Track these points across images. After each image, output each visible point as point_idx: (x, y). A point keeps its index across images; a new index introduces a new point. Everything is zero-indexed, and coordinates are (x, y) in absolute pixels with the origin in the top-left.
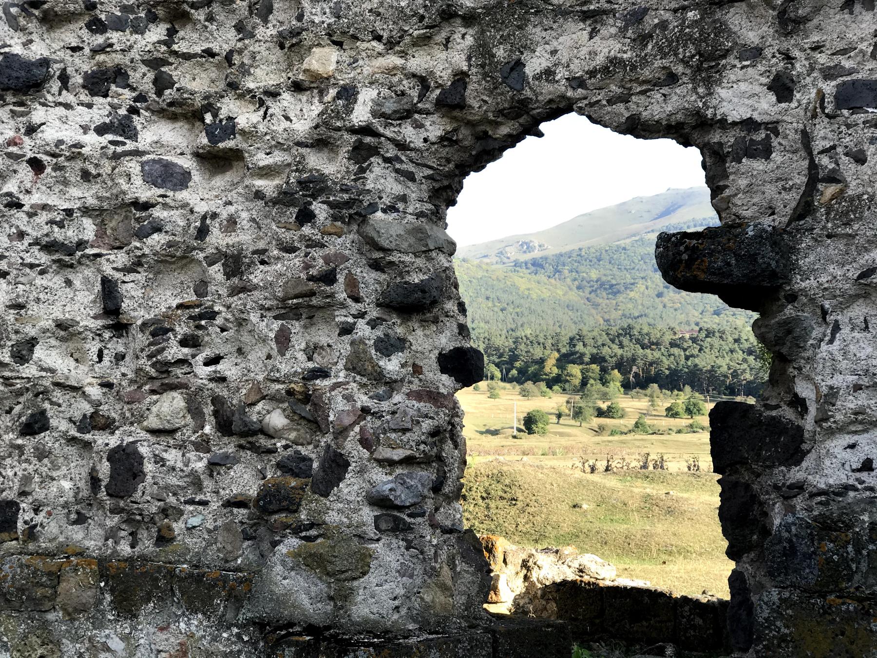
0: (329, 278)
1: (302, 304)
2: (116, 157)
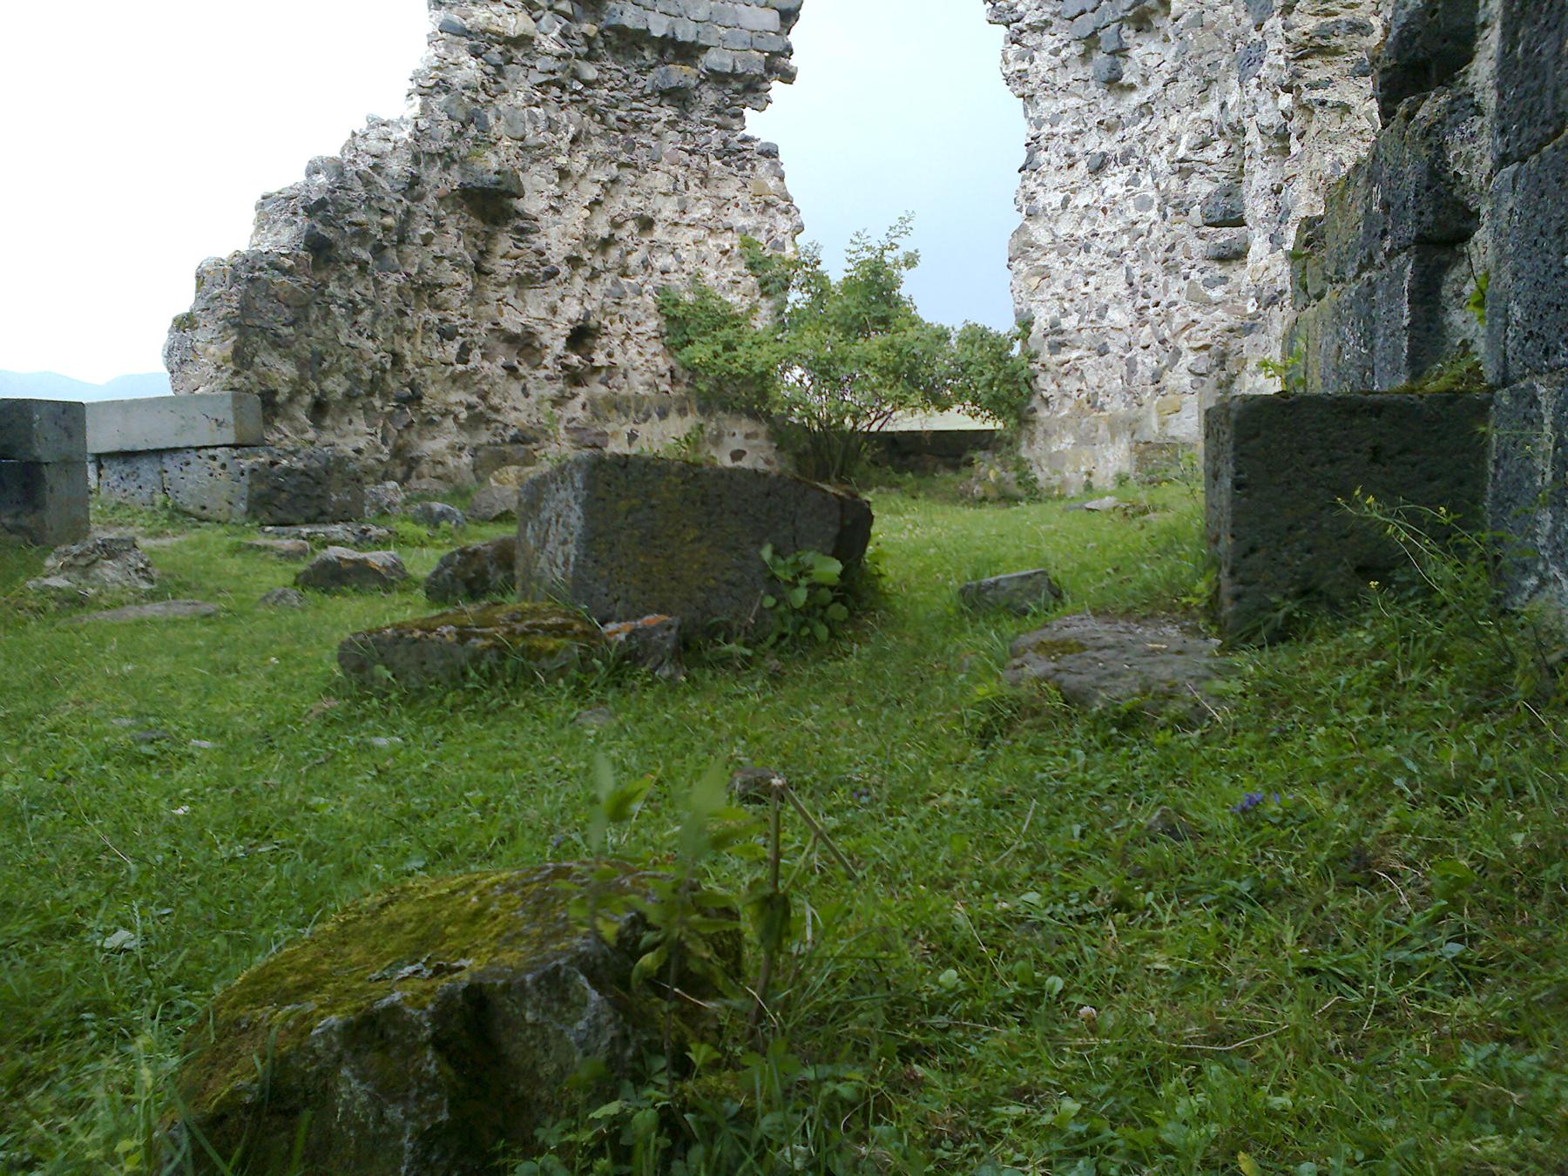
0: (1171, 248)
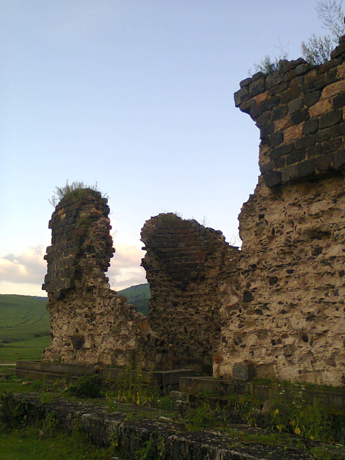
1: (207, 330)
2: (186, 313)
